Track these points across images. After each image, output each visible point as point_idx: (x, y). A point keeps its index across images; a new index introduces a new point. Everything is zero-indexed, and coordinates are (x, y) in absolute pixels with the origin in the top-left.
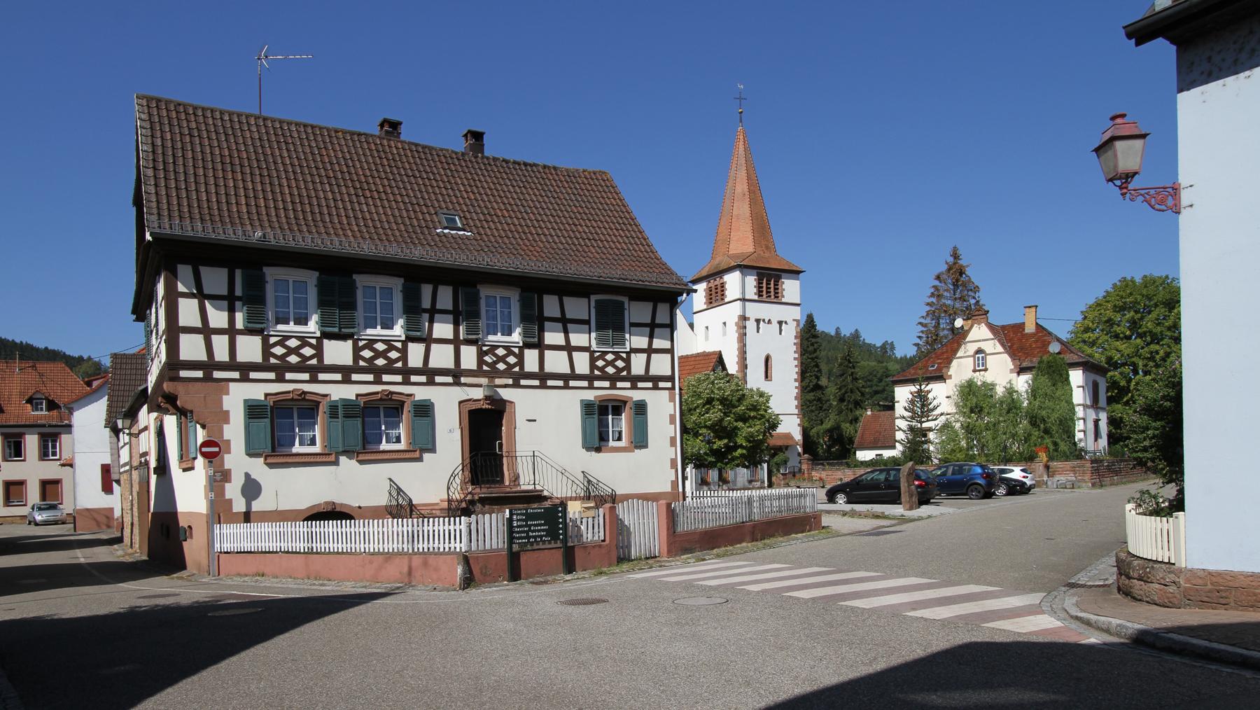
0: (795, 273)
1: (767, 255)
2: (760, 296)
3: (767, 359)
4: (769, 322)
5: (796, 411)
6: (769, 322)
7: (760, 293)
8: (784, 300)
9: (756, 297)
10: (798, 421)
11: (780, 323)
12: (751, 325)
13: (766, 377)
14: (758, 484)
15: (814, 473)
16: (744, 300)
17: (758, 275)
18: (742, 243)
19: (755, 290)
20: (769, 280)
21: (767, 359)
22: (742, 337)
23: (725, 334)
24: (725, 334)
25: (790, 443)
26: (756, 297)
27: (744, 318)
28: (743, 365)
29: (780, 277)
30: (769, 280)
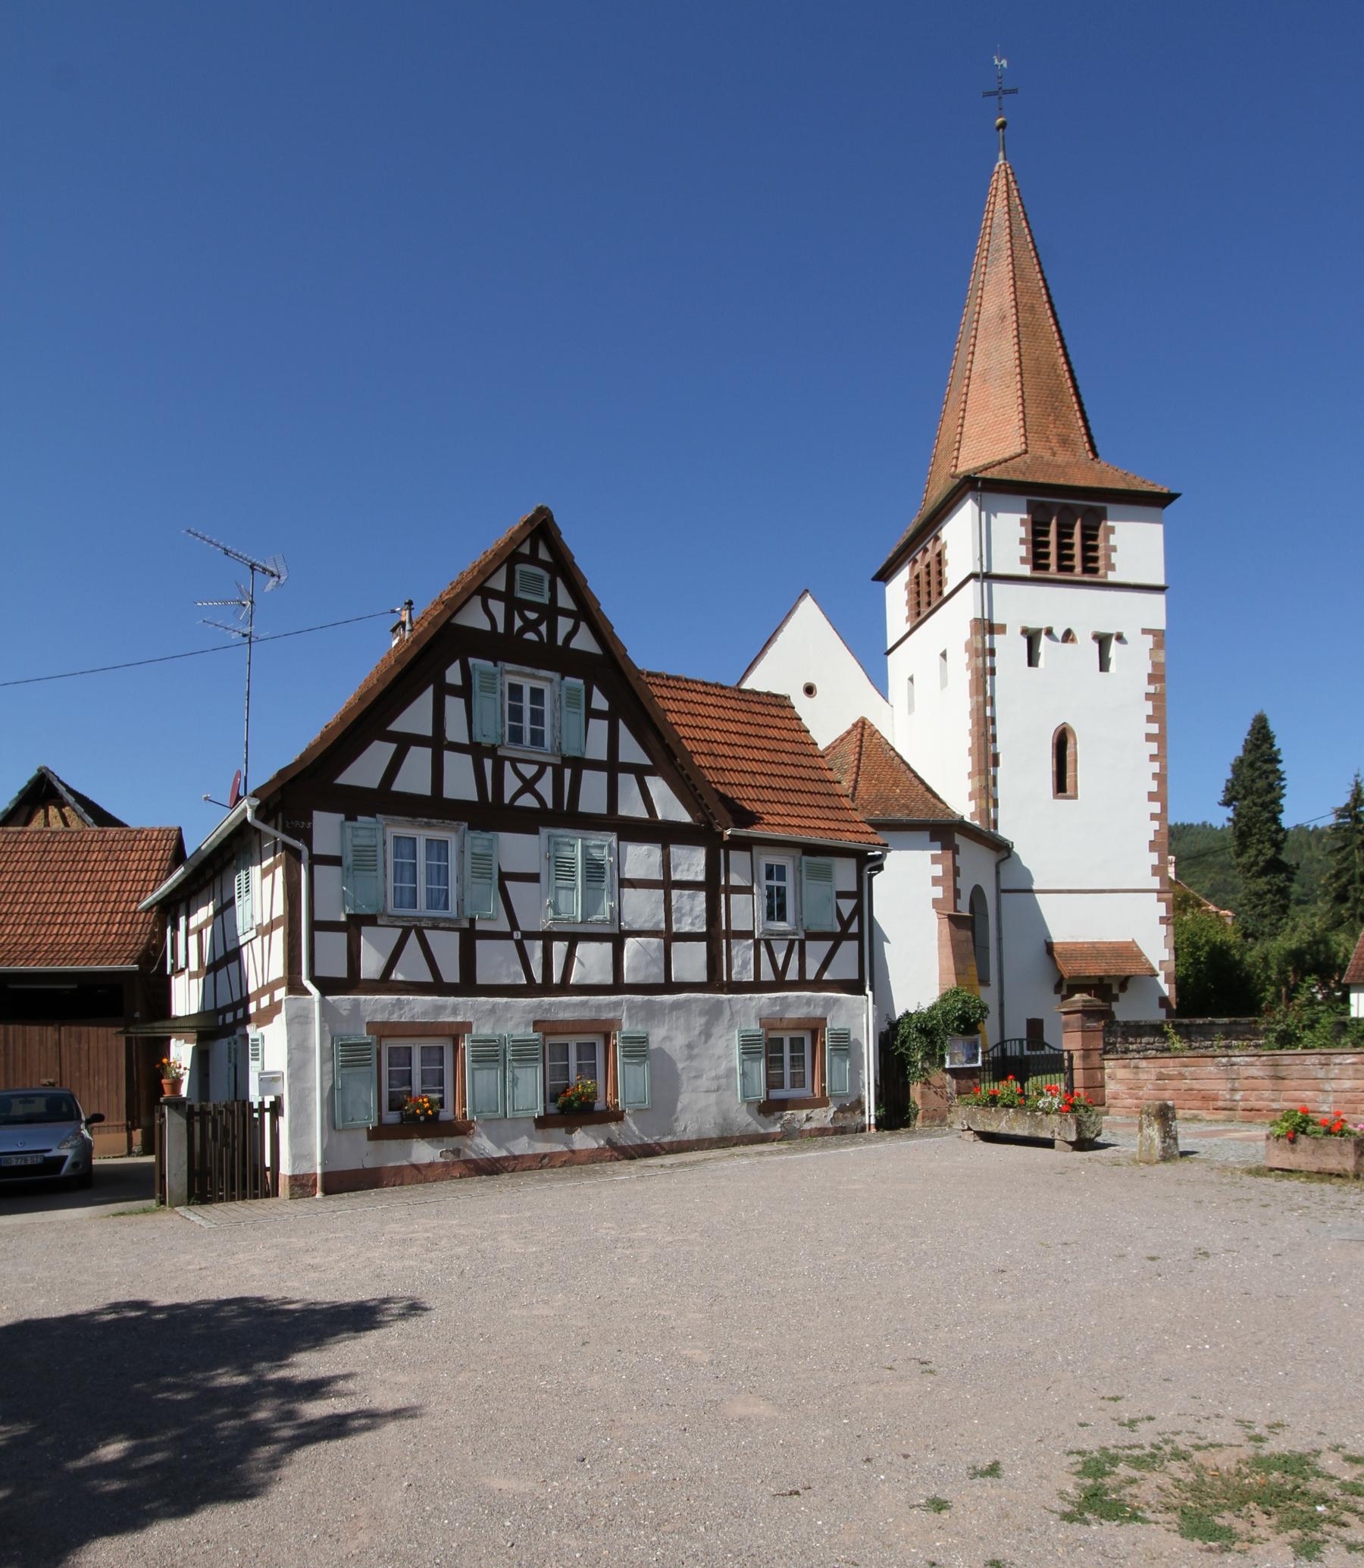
1: (1062, 458)
2: (1036, 567)
3: (1062, 742)
4: (1068, 636)
6: (1068, 636)
7: (1038, 558)
8: (1112, 577)
9: (1026, 570)
11: (1103, 641)
13: (1061, 785)
14: (823, 1116)
15: (1110, 1065)
17: (1031, 509)
18: (990, 425)
19: (1023, 551)
20: (1066, 528)
21: (1062, 742)
22: (984, 675)
25: (1130, 969)
26: (1026, 570)
30: (1066, 528)
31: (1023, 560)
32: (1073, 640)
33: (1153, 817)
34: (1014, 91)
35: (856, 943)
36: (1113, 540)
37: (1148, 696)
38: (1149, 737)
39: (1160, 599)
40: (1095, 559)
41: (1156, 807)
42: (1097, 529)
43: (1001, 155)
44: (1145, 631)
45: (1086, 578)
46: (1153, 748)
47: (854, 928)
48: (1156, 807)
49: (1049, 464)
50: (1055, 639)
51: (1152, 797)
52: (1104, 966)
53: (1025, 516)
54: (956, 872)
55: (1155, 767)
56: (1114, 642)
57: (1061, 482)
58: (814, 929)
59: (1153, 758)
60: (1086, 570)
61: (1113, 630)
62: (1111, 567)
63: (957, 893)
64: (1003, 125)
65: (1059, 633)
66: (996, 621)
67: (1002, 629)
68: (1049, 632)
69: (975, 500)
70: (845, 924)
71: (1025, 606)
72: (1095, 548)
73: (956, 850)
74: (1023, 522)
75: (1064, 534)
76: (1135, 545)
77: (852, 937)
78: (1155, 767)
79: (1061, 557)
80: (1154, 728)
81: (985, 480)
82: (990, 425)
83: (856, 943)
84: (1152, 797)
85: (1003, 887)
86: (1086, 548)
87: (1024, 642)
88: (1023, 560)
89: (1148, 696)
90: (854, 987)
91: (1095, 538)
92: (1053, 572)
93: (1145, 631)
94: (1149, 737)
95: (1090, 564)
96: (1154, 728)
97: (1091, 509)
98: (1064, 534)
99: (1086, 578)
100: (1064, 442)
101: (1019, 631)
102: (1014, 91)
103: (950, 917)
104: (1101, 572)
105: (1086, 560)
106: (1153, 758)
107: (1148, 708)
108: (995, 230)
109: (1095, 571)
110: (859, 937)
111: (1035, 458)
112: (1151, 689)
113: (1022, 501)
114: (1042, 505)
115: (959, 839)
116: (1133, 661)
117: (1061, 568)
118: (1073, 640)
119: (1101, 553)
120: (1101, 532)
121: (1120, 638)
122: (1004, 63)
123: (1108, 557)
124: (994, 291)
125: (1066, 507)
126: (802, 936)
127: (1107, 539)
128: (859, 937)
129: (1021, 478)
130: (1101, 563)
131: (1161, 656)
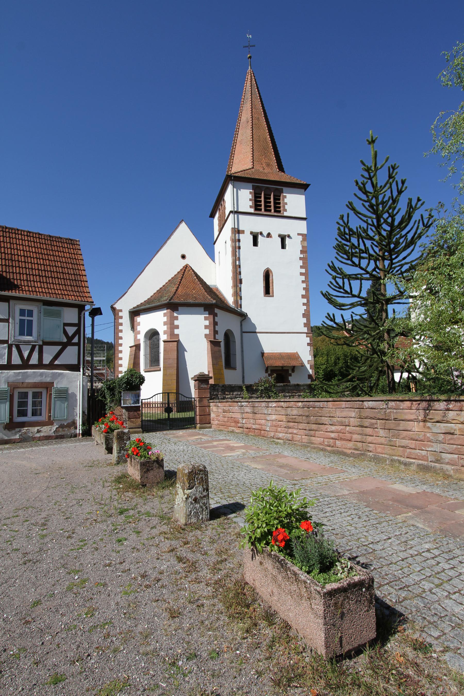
0: (302, 187)
2: (256, 209)
3: (267, 276)
4: (269, 235)
5: (305, 330)
6: (269, 235)
7: (257, 206)
8: (286, 214)
9: (252, 210)
10: (308, 340)
11: (283, 239)
12: (246, 240)
16: (237, 212)
17: (254, 188)
21: (267, 276)
23: (226, 254)
24: (226, 254)
27: (237, 231)
28: (237, 281)
29: (281, 191)
31: (251, 207)
32: (271, 237)
33: (304, 304)
34: (254, 46)
35: (77, 347)
36: (286, 200)
37: (301, 258)
38: (301, 274)
39: (304, 223)
40: (280, 208)
41: (305, 301)
42: (280, 196)
43: (250, 67)
44: (299, 234)
45: (276, 214)
46: (303, 278)
47: (76, 340)
48: (305, 301)
49: (261, 172)
50: (264, 236)
51: (303, 297)
52: (283, 362)
53: (252, 191)
54: (215, 324)
55: (304, 285)
56: (287, 238)
57: (265, 178)
58: (47, 340)
59: (303, 282)
60: (275, 211)
61: (286, 234)
62: (286, 210)
63: (216, 332)
64: (250, 57)
65: (265, 234)
66: (240, 229)
67: (243, 232)
68: (261, 233)
69: (232, 184)
70: (69, 339)
71: (251, 224)
72: (279, 203)
73: (215, 315)
74: (250, 193)
75: (267, 198)
76: (294, 203)
77: (74, 344)
78: (304, 285)
79: (266, 206)
80: (303, 271)
81: (235, 177)
82: (242, 160)
83: (77, 347)
84: (303, 297)
85: (244, 331)
86: (275, 203)
87: (251, 237)
88: (251, 207)
89: (301, 258)
90: (75, 368)
91: (279, 200)
92: (263, 212)
93: (299, 234)
94: (301, 274)
95: (277, 209)
96: (303, 271)
97: (277, 189)
98: (267, 198)
99: (276, 214)
100: (268, 165)
101: (249, 233)
102: (254, 46)
103: (211, 341)
104: (282, 212)
105: (275, 207)
106: (303, 282)
107: (301, 263)
108: (247, 92)
109: (279, 212)
110: (78, 344)
111: (256, 170)
112: (302, 256)
113: (250, 185)
114: (258, 186)
115: (217, 311)
116: (295, 245)
117: (266, 210)
118: (271, 237)
119: (281, 205)
120: (281, 198)
121: (289, 236)
122: (251, 36)
123: (284, 207)
124: (246, 115)
125: (267, 188)
126: (41, 343)
127: (283, 200)
128: (78, 344)
129: (249, 176)
130: (282, 209)
131: (305, 244)
